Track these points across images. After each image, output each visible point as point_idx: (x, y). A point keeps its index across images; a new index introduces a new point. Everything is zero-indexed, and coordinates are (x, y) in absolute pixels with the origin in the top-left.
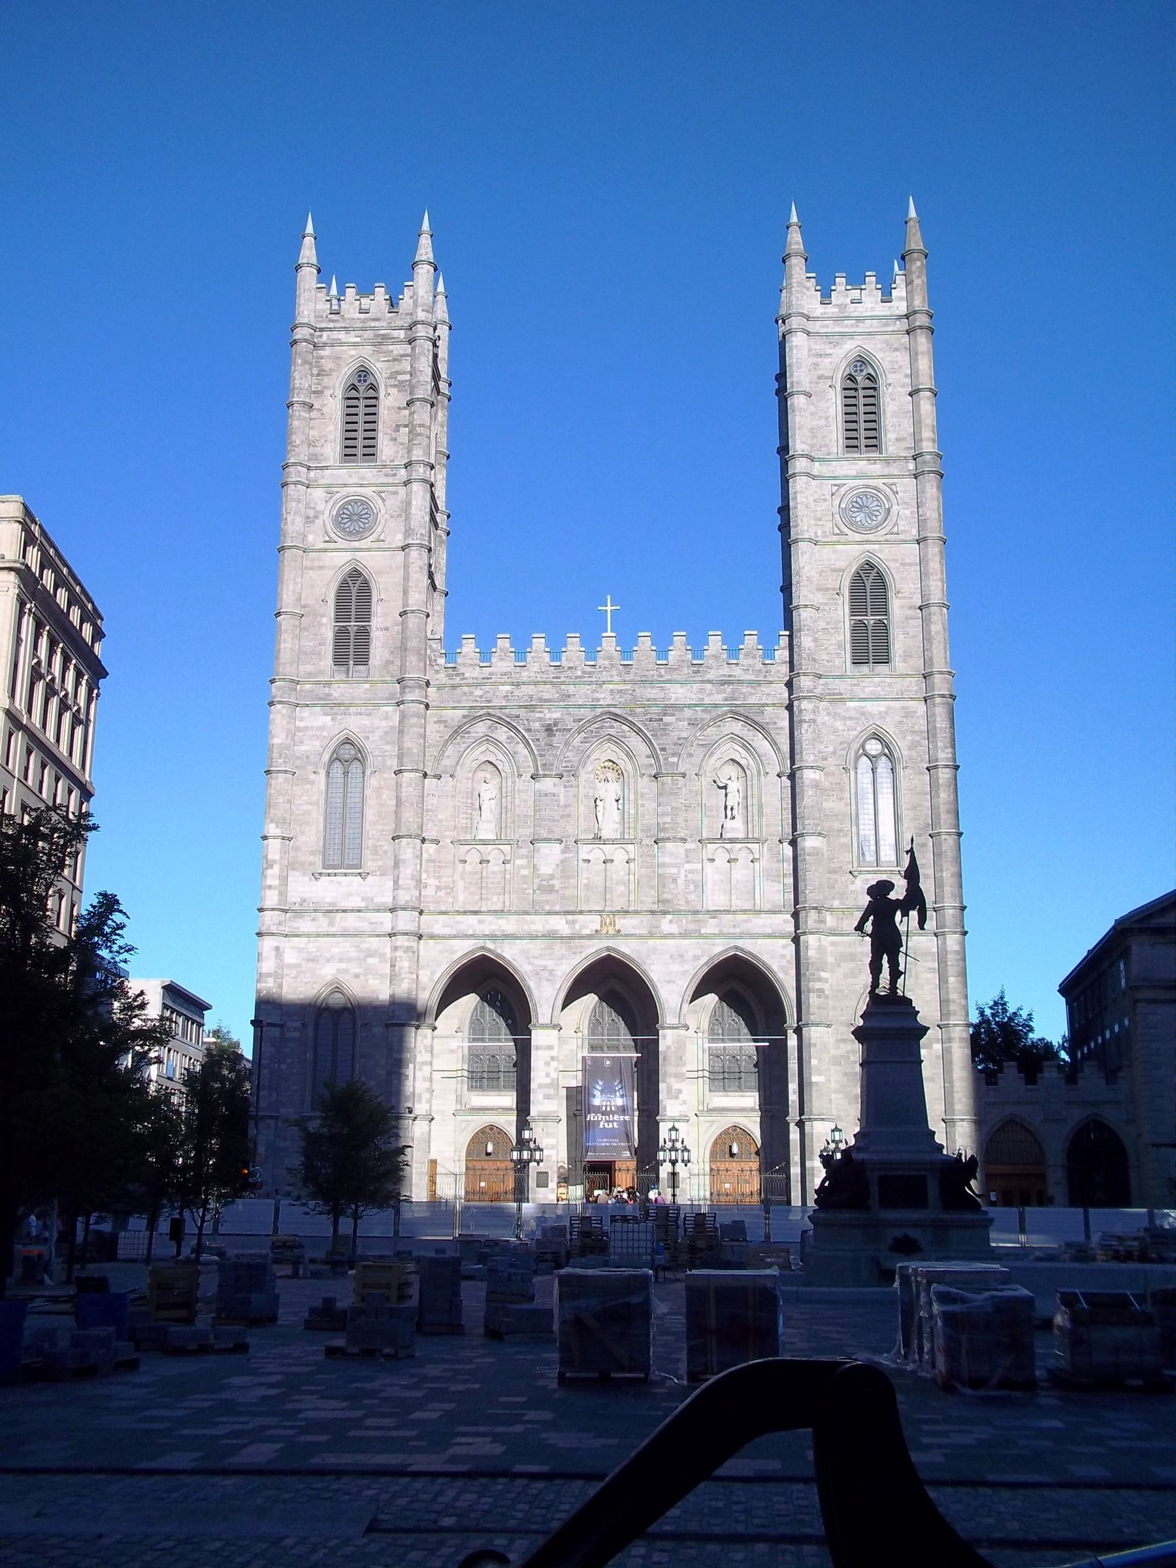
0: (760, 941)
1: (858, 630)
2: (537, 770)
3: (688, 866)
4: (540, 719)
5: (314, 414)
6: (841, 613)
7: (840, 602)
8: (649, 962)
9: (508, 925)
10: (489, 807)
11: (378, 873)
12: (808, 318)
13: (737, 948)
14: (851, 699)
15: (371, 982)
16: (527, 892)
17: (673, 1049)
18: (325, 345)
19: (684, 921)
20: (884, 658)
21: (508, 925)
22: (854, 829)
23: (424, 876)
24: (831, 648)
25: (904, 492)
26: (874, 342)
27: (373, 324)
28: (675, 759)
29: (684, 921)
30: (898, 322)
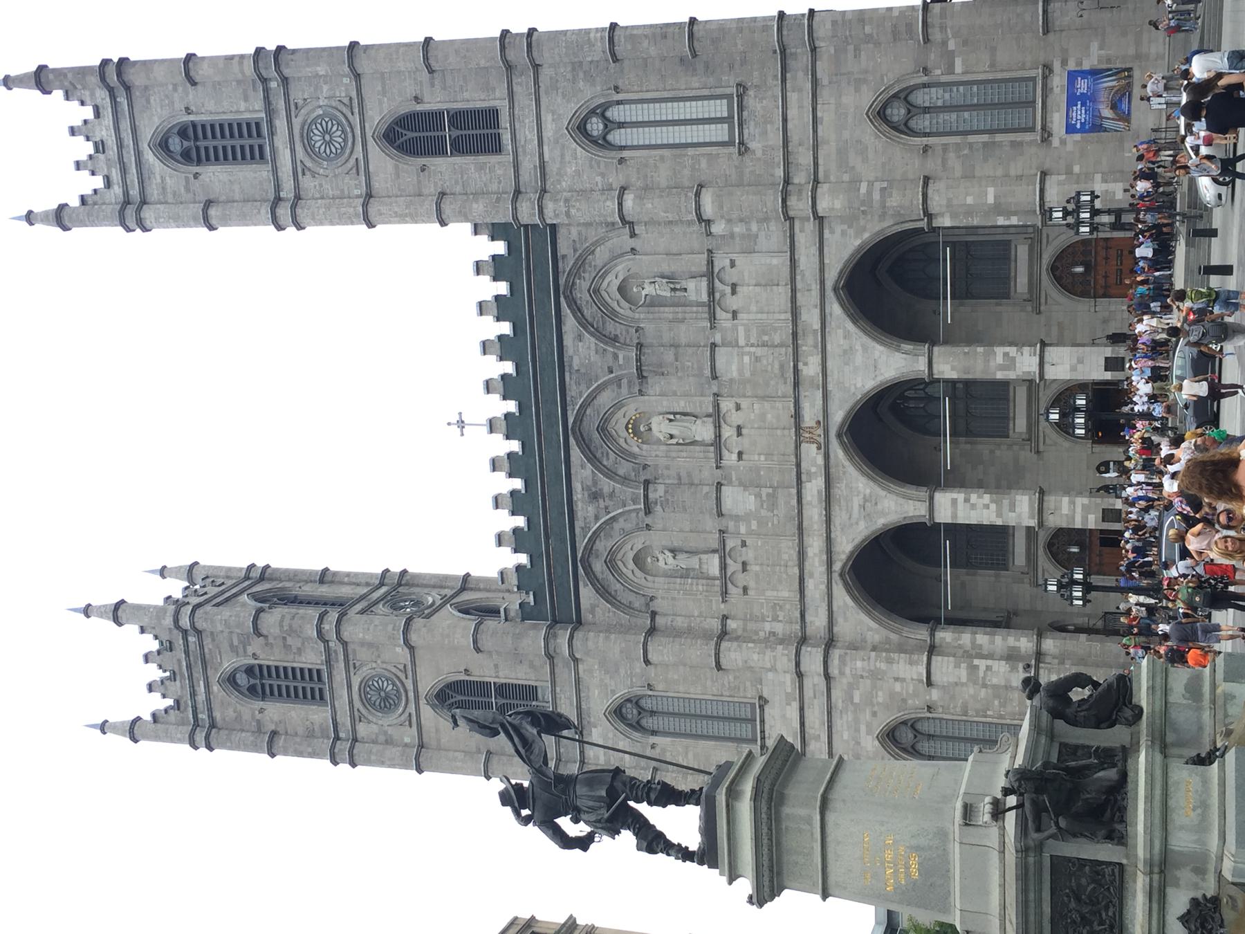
0: (826, 261)
1: (460, 148)
2: (641, 508)
3: (742, 342)
5: (281, 729)
6: (445, 167)
7: (433, 168)
9: (815, 546)
10: (683, 562)
11: (759, 687)
12: (127, 202)
13: (835, 289)
14: (541, 155)
15: (880, 700)
16: (776, 522)
17: (956, 364)
18: (211, 716)
19: (804, 348)
20: (490, 117)
21: (815, 546)
22: (691, 151)
23: (762, 634)
24: (484, 179)
25: (303, 91)
26: (142, 127)
27: (184, 668)
28: (621, 357)
29: (804, 348)
30: (118, 100)
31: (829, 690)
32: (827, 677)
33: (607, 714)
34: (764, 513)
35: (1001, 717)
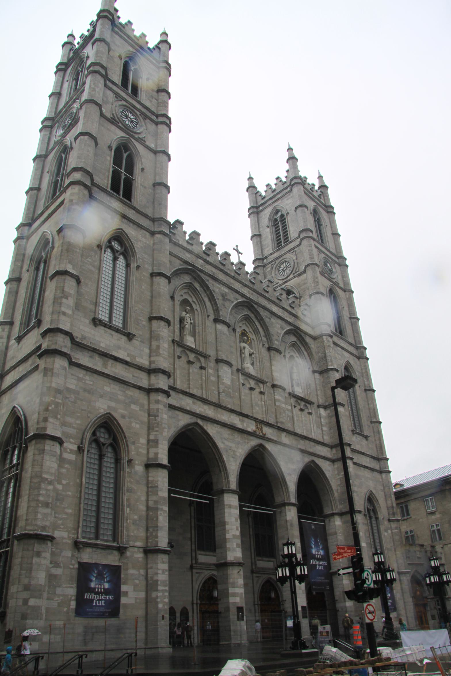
4: (219, 289)
11: (139, 339)
15: (133, 424)
31: (140, 388)
32: (149, 391)
33: (121, 230)
35: (127, 520)
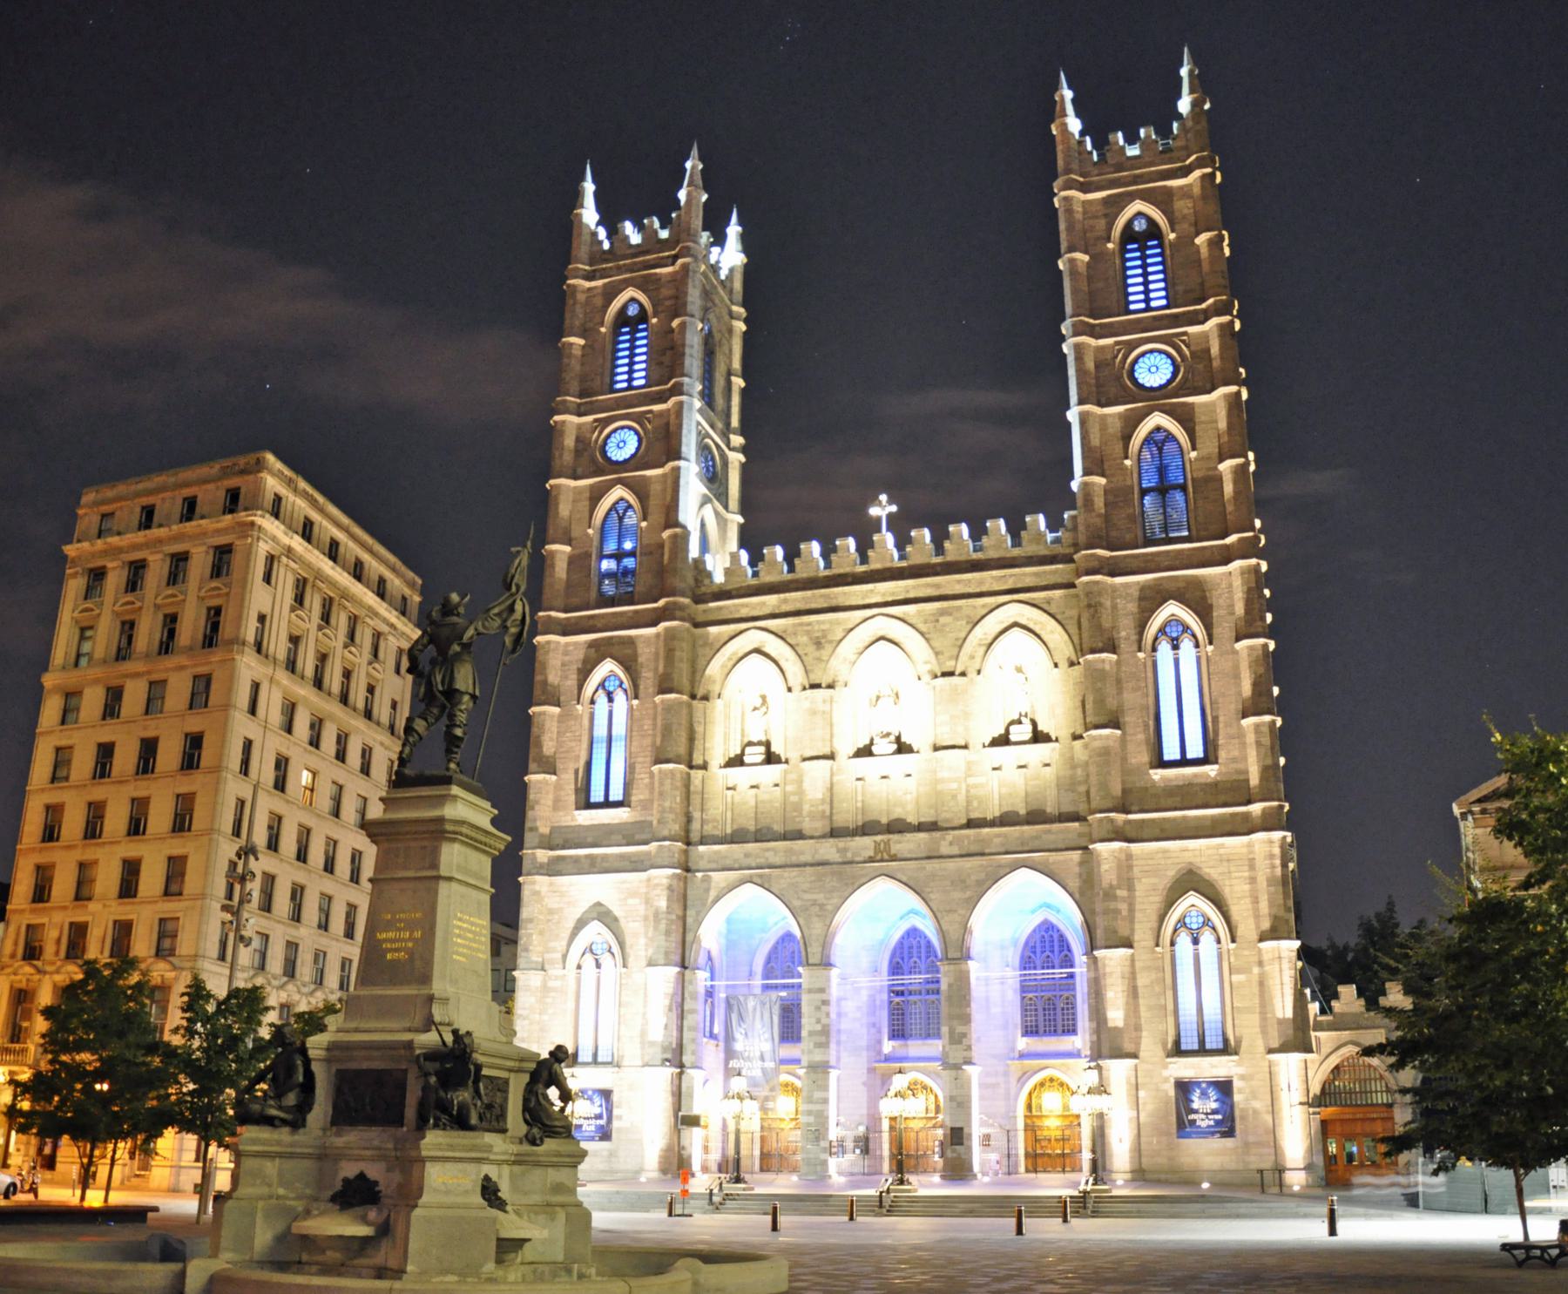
8: (928, 890)
34: (806, 807)
